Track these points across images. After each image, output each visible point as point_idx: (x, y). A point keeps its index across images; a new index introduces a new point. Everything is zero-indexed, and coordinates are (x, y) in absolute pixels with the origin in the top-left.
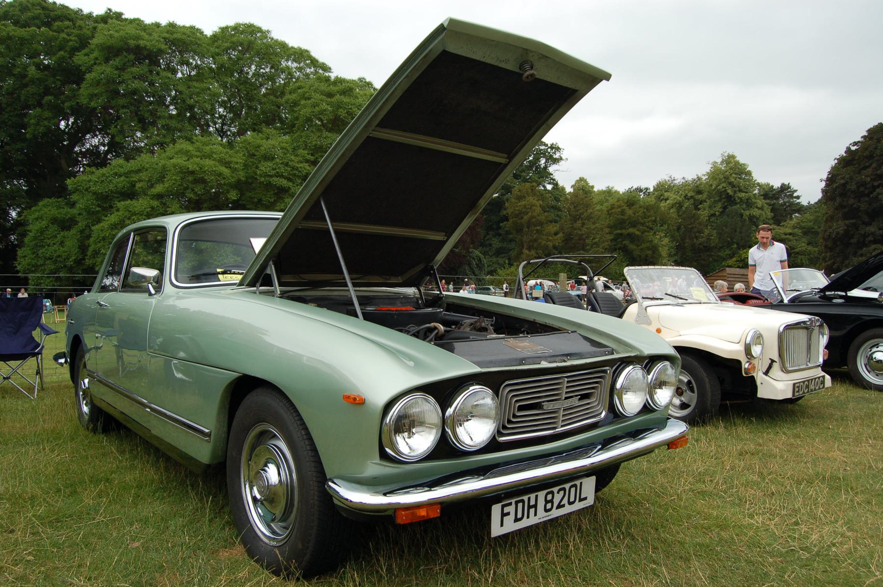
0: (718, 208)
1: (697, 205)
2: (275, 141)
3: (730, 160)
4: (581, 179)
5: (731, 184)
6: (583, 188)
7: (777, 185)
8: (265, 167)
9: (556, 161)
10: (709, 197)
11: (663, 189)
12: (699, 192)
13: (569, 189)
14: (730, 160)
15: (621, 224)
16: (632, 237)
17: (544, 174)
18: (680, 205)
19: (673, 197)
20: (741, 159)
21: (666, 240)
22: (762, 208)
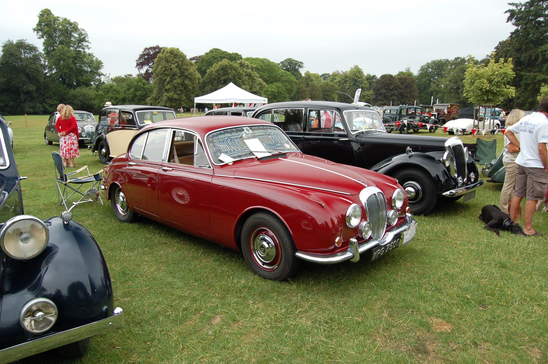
0: (352, 83)
1: (346, 82)
2: (279, 84)
3: (356, 67)
4: (308, 72)
5: (357, 76)
6: (308, 74)
7: (372, 75)
8: (280, 89)
9: (301, 67)
10: (350, 80)
11: (335, 75)
12: (346, 77)
13: (303, 75)
14: (356, 67)
15: (324, 91)
16: (327, 95)
17: (297, 70)
18: (340, 82)
19: (338, 79)
20: (360, 67)
21: (337, 96)
22: (365, 84)
